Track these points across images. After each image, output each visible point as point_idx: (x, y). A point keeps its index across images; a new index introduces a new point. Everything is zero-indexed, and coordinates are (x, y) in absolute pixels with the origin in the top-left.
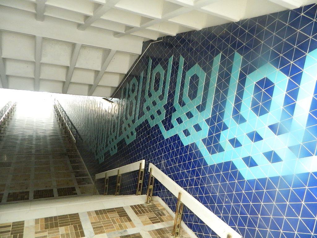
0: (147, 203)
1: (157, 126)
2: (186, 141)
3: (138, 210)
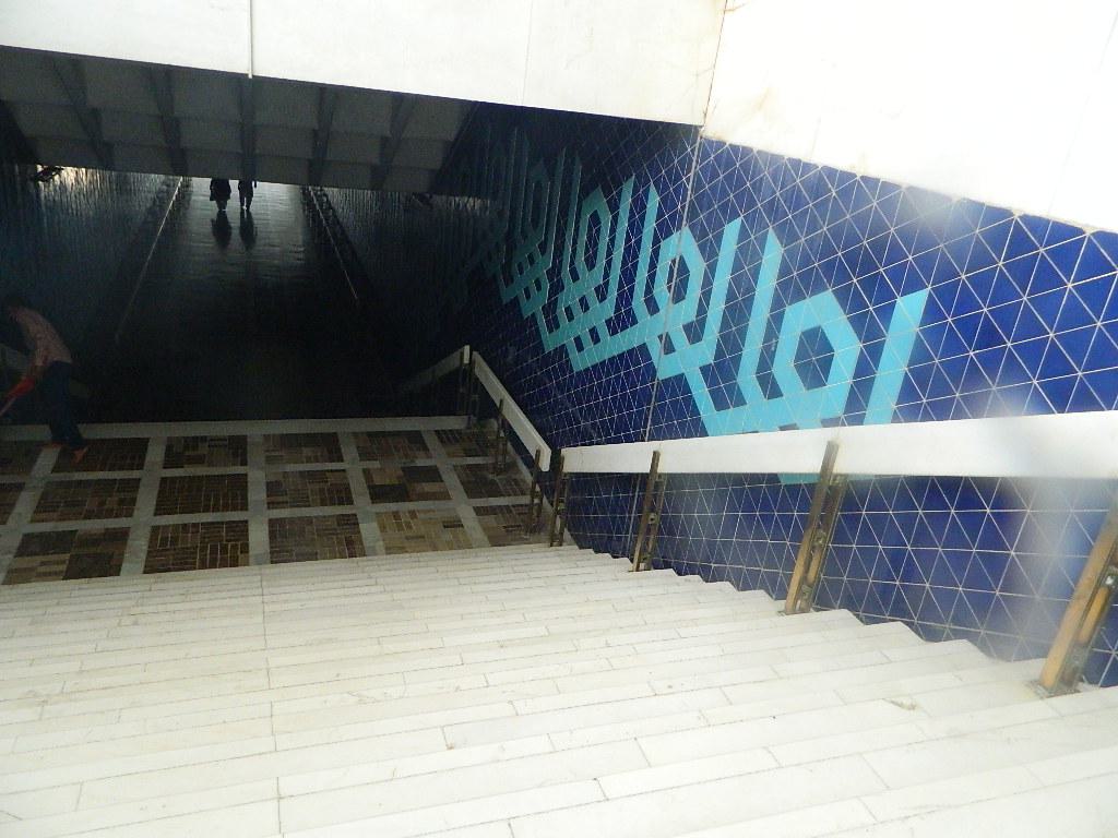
0: (468, 428)
1: (494, 278)
2: (527, 314)
3: (445, 437)
